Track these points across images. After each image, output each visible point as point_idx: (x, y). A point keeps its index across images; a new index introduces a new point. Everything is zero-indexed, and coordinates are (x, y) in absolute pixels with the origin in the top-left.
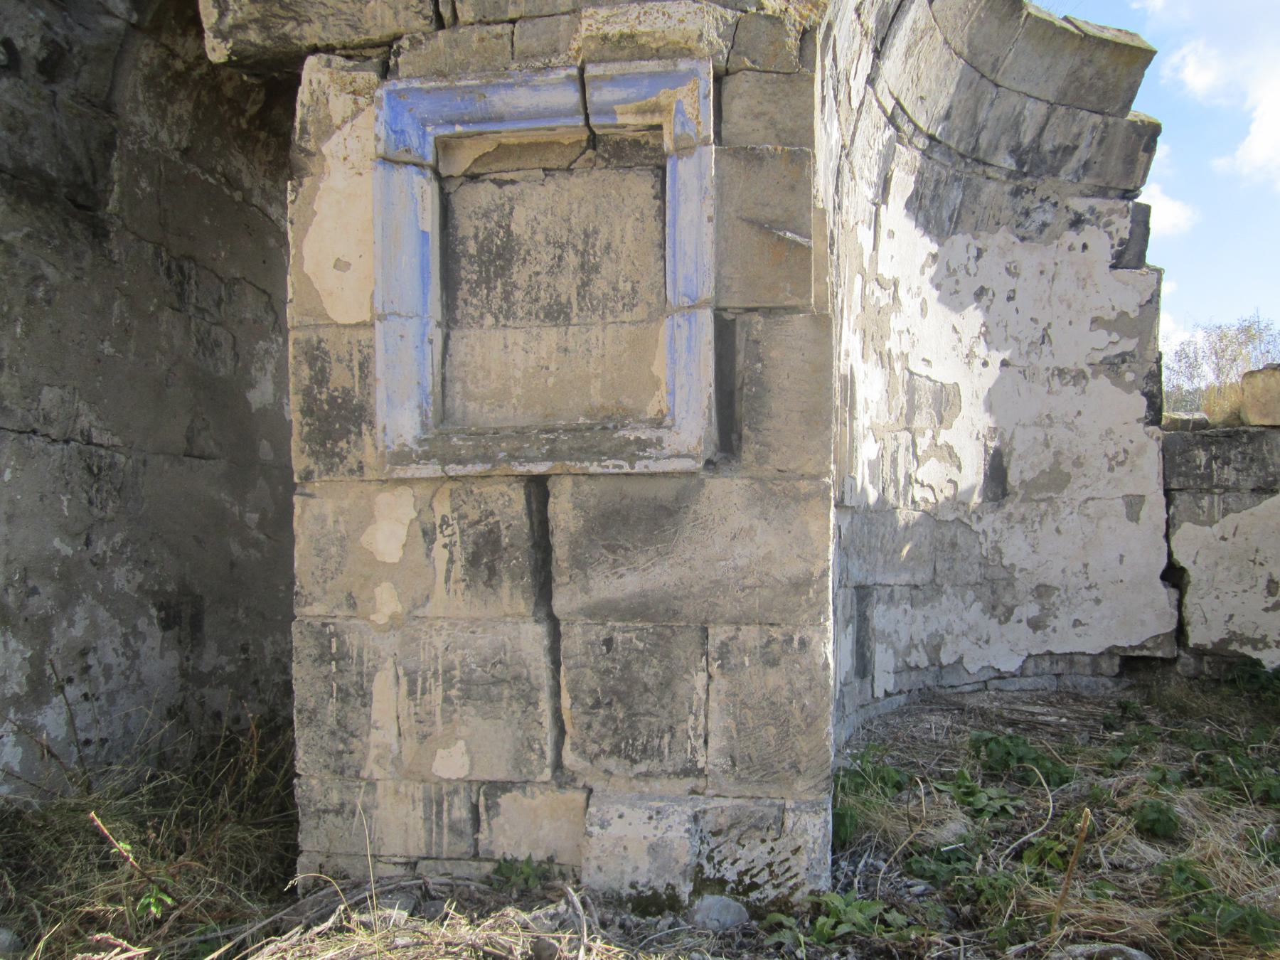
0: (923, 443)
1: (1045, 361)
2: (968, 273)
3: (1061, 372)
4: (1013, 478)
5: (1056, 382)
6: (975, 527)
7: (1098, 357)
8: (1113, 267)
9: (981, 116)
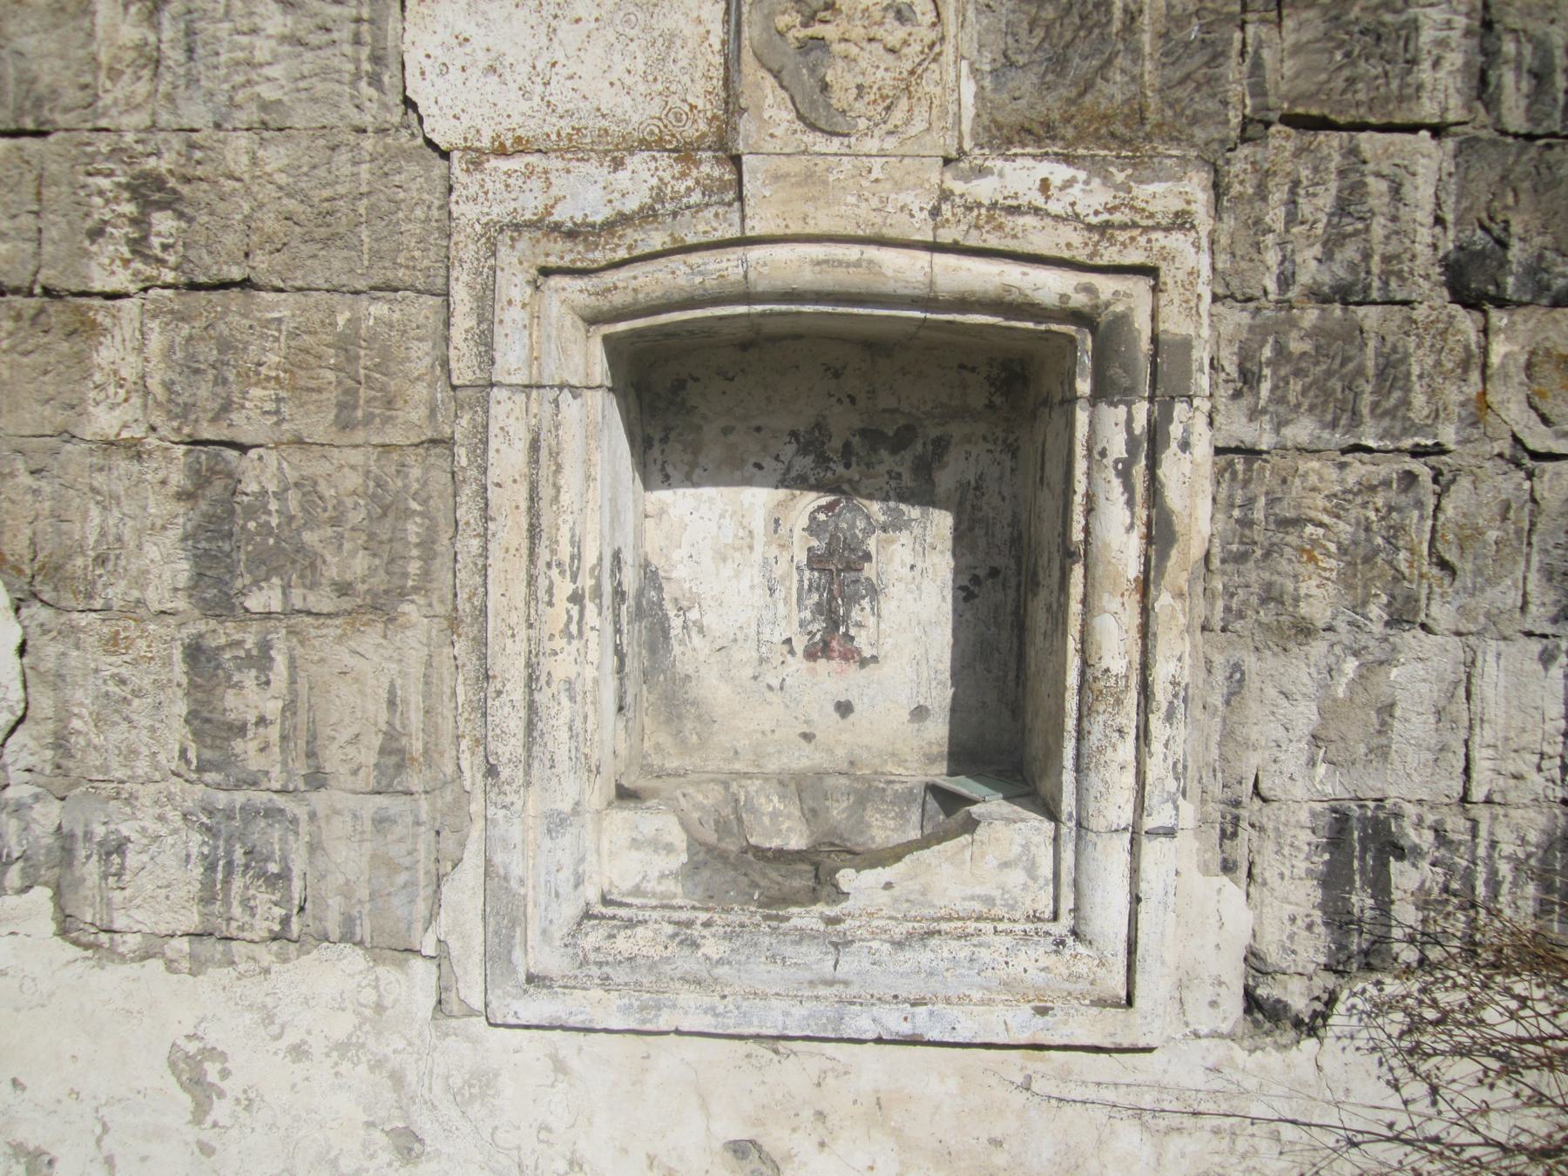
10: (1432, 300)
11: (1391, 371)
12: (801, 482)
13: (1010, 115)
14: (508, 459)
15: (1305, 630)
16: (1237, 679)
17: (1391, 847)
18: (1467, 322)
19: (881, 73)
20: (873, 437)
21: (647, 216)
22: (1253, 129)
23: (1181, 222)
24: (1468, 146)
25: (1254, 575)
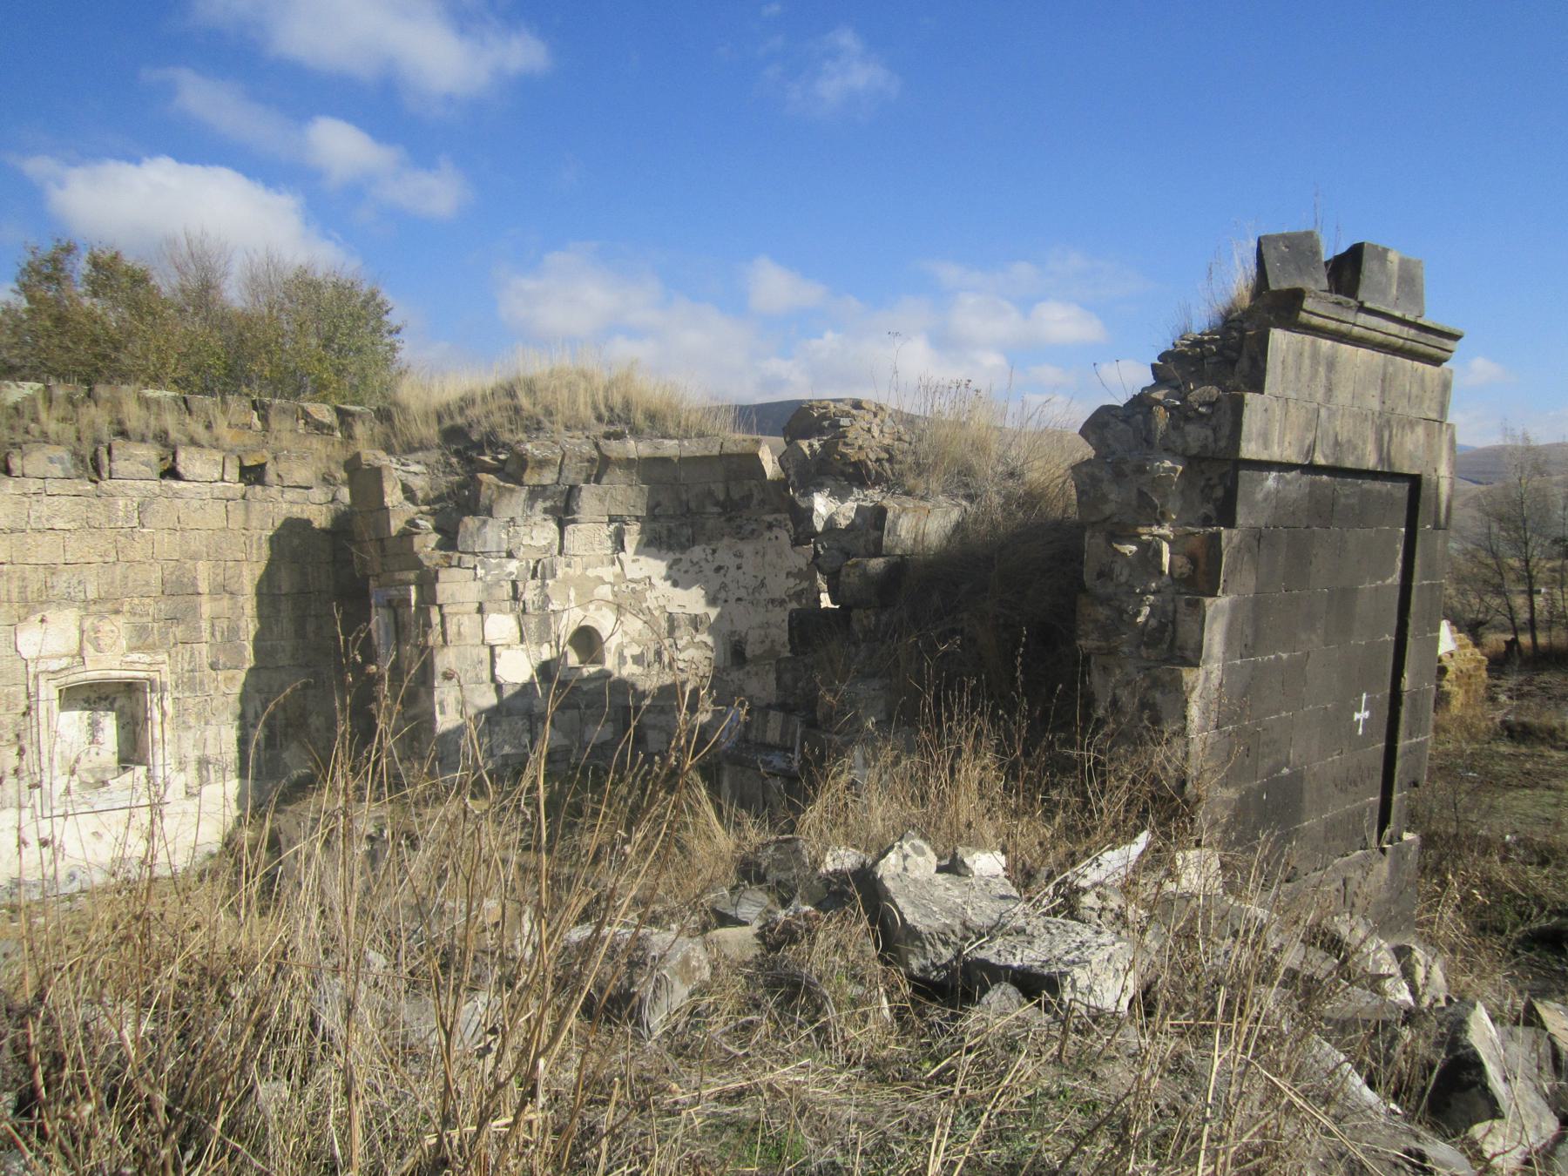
0: (681, 643)
1: (764, 595)
2: (707, 560)
3: (773, 601)
4: (749, 653)
5: (770, 606)
6: (725, 678)
7: (792, 592)
8: (793, 546)
9: (684, 497)
10: (208, 670)
11: (202, 683)
12: (85, 709)
13: (132, 645)
14: (43, 713)
15: (190, 727)
16: (179, 737)
17: (208, 763)
18: (213, 673)
19: (109, 642)
20: (100, 698)
21: (66, 669)
22: (175, 644)
23: (164, 663)
24: (211, 645)
25: (181, 719)
